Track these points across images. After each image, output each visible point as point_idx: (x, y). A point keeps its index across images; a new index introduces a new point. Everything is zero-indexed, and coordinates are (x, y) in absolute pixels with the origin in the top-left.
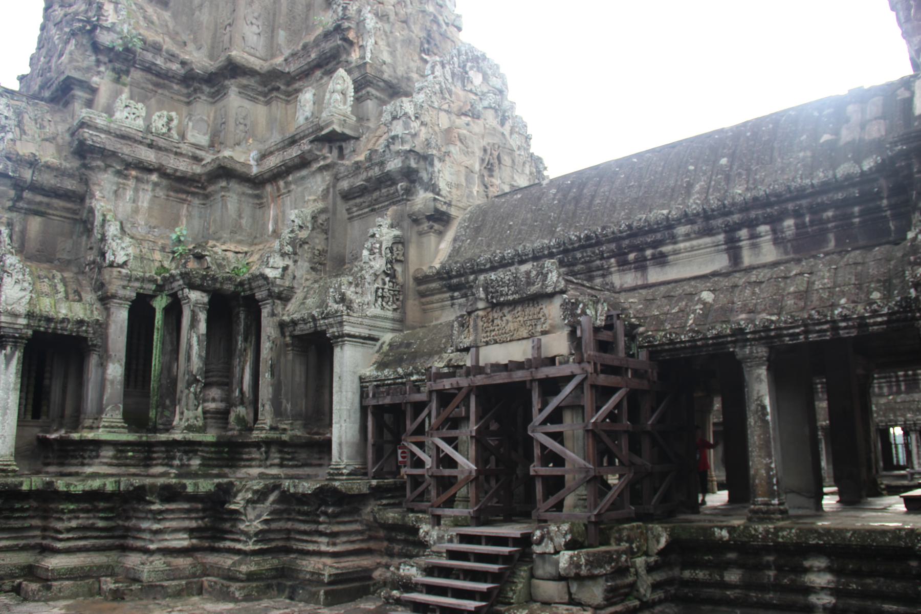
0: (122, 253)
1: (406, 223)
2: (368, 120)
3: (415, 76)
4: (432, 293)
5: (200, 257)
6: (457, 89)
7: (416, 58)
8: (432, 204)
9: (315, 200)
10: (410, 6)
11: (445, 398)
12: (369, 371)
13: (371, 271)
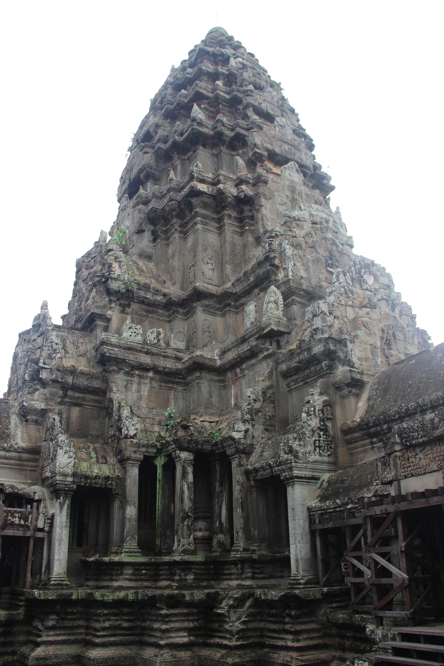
0: (133, 428)
1: (331, 390)
2: (295, 319)
3: (324, 284)
4: (356, 440)
5: (185, 428)
6: (357, 289)
7: (324, 271)
8: (349, 375)
9: (263, 380)
10: (315, 236)
11: (377, 522)
12: (314, 503)
13: (309, 428)
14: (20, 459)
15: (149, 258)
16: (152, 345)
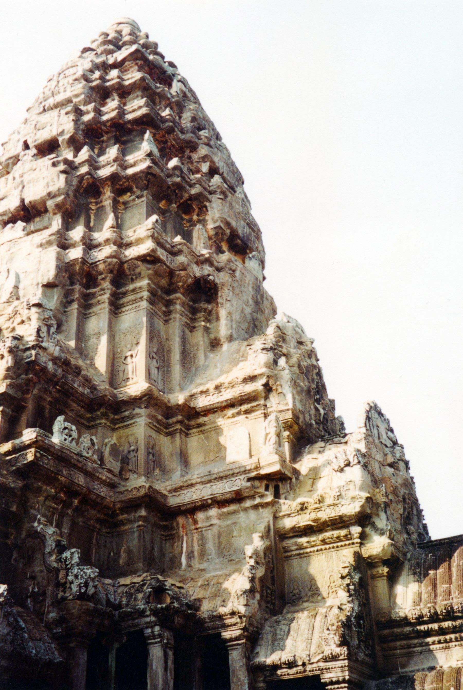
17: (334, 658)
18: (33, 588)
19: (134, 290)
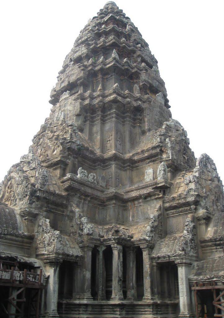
1: (195, 220)
4: (208, 246)
7: (182, 157)
8: (206, 214)
9: (157, 211)
13: (189, 239)
14: (23, 242)
15: (81, 130)
16: (92, 183)
17: (179, 255)
18: (73, 230)
19: (110, 114)
